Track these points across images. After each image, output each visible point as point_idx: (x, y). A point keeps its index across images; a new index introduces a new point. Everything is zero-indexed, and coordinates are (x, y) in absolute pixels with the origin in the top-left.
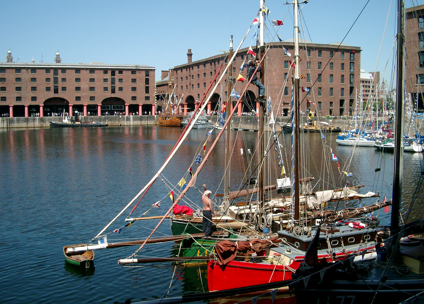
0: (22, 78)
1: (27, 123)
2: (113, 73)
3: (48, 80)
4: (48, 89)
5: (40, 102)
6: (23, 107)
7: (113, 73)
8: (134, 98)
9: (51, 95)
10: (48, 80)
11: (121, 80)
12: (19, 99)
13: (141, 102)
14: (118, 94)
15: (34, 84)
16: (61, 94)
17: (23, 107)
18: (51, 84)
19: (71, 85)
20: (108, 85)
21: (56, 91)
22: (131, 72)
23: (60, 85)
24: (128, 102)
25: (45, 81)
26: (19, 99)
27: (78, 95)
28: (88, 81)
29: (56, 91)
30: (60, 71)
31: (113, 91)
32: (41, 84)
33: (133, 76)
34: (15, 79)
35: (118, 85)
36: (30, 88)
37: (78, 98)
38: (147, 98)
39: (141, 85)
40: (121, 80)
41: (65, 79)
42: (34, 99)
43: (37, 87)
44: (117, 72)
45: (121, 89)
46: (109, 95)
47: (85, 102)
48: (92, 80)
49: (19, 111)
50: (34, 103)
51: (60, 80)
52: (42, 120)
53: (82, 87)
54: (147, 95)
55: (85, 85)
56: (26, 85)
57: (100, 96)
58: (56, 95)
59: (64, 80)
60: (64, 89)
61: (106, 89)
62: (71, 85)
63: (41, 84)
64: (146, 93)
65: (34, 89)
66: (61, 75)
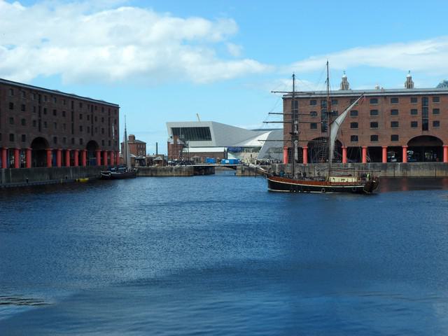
0: (380, 111)
1: (386, 172)
3: (414, 112)
4: (414, 124)
5: (403, 142)
6: (380, 149)
9: (418, 132)
10: (414, 112)
12: (374, 138)
15: (396, 119)
16: (432, 132)
17: (380, 149)
18: (419, 118)
21: (425, 127)
23: (432, 118)
25: (410, 114)
26: (374, 138)
29: (425, 127)
30: (430, 99)
32: (405, 119)
34: (369, 112)
36: (389, 124)
41: (438, 110)
42: (395, 138)
43: (399, 121)
49: (375, 154)
50: (395, 144)
51: (430, 111)
52: (405, 167)
56: (384, 121)
58: (425, 133)
59: (436, 111)
60: (436, 124)
63: (405, 119)
65: (394, 124)
66: (432, 105)
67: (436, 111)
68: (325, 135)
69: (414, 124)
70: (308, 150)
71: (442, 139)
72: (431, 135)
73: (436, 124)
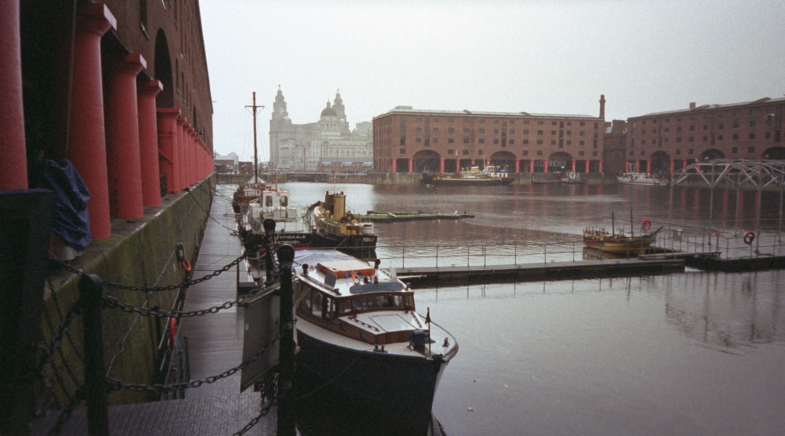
2: (562, 125)
7: (562, 125)
8: (581, 153)
9: (499, 148)
10: (496, 131)
11: (569, 133)
12: (466, 152)
13: (588, 158)
14: (565, 149)
16: (508, 148)
18: (499, 137)
19: (519, 137)
20: (556, 138)
22: (579, 124)
23: (509, 137)
24: (576, 157)
26: (466, 152)
27: (526, 149)
28: (537, 133)
29: (504, 145)
30: (509, 121)
31: (561, 145)
33: (582, 128)
35: (566, 137)
37: (526, 153)
38: (595, 153)
39: (589, 139)
40: (569, 133)
44: (566, 124)
45: (569, 143)
46: (556, 149)
47: (532, 157)
48: (540, 132)
53: (530, 140)
54: (595, 150)
55: (533, 138)
57: (548, 149)
58: (504, 149)
59: (513, 132)
60: (512, 142)
61: (553, 142)
62: (519, 137)
64: (594, 147)
66: (509, 127)
67: (513, 132)
68: (427, 148)
69: (496, 142)
70: (413, 161)
71: (516, 154)
72: (508, 150)
73: (512, 142)
